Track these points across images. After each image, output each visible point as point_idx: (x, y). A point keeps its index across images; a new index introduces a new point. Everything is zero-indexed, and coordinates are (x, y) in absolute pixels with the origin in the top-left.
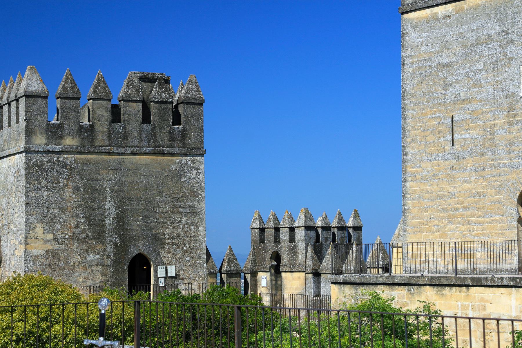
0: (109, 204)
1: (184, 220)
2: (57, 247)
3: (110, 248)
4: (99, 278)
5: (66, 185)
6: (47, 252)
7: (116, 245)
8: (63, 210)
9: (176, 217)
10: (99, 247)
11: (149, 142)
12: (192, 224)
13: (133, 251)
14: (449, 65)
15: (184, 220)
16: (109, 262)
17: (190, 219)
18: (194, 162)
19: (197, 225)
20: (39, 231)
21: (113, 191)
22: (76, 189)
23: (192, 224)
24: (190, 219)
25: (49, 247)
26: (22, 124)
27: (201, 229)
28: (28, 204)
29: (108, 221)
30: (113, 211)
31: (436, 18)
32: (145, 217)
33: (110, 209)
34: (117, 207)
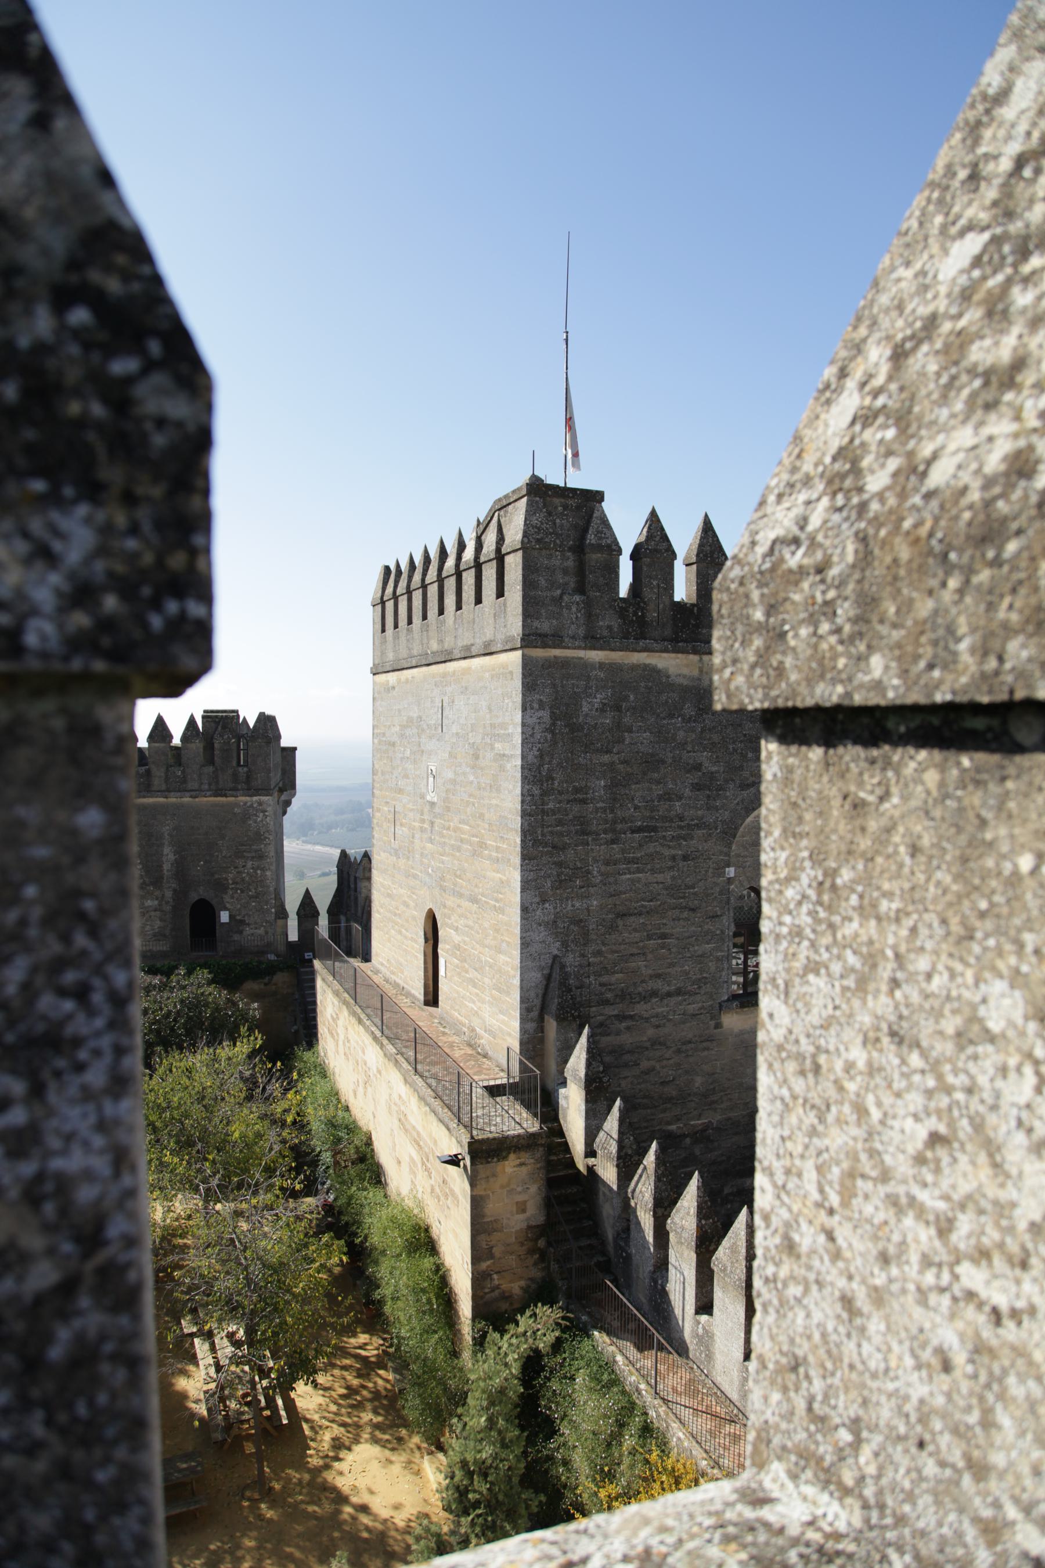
0: (167, 850)
1: (250, 864)
3: (169, 894)
4: (158, 923)
7: (175, 891)
9: (240, 862)
10: (157, 893)
11: (210, 784)
12: (258, 868)
13: (194, 897)
15: (250, 864)
16: (168, 908)
17: (256, 864)
19: (263, 870)
21: (171, 835)
23: (258, 868)
24: (256, 864)
27: (268, 873)
29: (166, 867)
32: (206, 862)
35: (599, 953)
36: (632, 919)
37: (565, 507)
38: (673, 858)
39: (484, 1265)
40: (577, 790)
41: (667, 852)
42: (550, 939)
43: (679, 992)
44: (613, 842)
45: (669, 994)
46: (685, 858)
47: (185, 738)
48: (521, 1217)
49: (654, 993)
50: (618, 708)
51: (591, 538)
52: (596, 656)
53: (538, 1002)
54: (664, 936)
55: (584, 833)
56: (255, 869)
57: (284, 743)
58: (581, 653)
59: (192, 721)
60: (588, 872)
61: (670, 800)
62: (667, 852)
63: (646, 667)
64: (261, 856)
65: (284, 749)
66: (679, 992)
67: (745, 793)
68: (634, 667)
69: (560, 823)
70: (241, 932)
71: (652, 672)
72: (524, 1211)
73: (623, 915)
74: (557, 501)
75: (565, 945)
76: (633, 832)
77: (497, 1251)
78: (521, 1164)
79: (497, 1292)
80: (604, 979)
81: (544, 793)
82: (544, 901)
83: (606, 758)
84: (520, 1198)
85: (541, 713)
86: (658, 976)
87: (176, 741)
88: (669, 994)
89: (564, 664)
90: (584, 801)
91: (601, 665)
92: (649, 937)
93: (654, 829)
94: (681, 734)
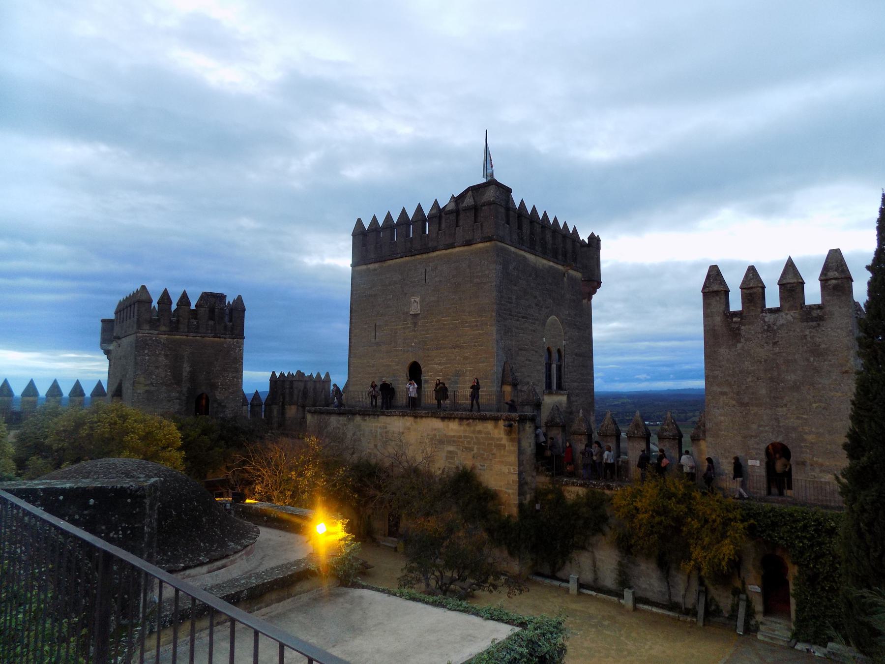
2: (153, 388)
3: (185, 390)
4: (177, 407)
6: (147, 391)
8: (157, 367)
14: (375, 295)
16: (184, 398)
18: (238, 343)
20: (142, 379)
22: (166, 356)
25: (147, 388)
26: (135, 319)
28: (136, 363)
29: (185, 374)
30: (188, 369)
31: (368, 269)
33: (186, 368)
34: (190, 367)
47: (196, 306)
52: (513, 249)
68: (521, 256)
73: (521, 350)
81: (502, 297)
83: (515, 288)
87: (193, 307)
90: (510, 303)
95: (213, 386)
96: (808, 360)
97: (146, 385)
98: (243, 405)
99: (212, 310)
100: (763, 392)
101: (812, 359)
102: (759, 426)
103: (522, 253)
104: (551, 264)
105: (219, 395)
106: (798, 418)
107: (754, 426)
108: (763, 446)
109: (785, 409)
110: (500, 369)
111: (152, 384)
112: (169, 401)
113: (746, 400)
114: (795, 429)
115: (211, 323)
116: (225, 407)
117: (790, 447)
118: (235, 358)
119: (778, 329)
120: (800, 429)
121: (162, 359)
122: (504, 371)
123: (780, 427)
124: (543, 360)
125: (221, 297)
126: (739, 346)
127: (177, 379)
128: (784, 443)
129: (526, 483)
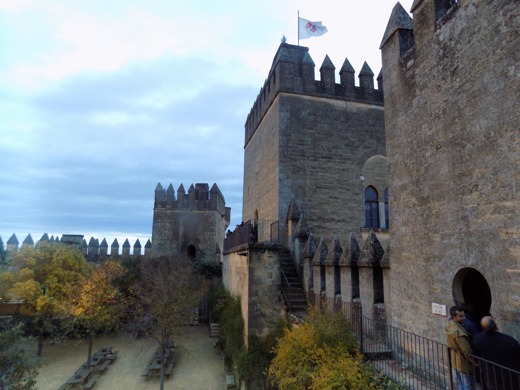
2: (162, 242)
3: (180, 243)
5: (167, 221)
6: (159, 244)
8: (165, 230)
10: (177, 242)
13: (189, 245)
15: (208, 233)
16: (180, 248)
17: (210, 233)
18: (213, 213)
19: (213, 235)
22: (170, 223)
24: (210, 233)
25: (159, 242)
29: (180, 233)
35: (310, 200)
36: (323, 190)
37: (295, 52)
38: (339, 170)
39: (254, 299)
40: (300, 141)
41: (336, 167)
42: (290, 192)
43: (343, 221)
44: (315, 160)
45: (339, 221)
46: (344, 170)
47: (189, 191)
48: (270, 279)
49: (333, 220)
50: (315, 115)
51: (304, 60)
53: (286, 216)
54: (336, 198)
55: (303, 156)
56: (210, 235)
57: (226, 206)
58: (301, 96)
59: (192, 186)
60: (305, 170)
61: (337, 148)
62: (336, 167)
63: (325, 102)
64: (212, 231)
65: (226, 208)
66: (343, 221)
67: (366, 150)
68: (321, 102)
69: (294, 151)
70: (204, 257)
71: (329, 104)
72: (271, 277)
74: (292, 50)
75: (296, 195)
76: (322, 158)
77: (260, 293)
78: (270, 257)
79: (259, 312)
80: (313, 211)
81: (288, 140)
82: (288, 178)
83: (311, 131)
84: (270, 271)
85: (286, 113)
86: (335, 213)
87: (187, 193)
88: (339, 221)
89: (295, 99)
90: (303, 145)
91: (309, 100)
92: (330, 197)
93: (331, 158)
94: (340, 127)
95: (198, 241)
96: (505, 75)
97: (158, 240)
98: (217, 253)
99: (197, 194)
100: (445, 170)
101: (512, 70)
102: (443, 237)
103: (324, 100)
104: (373, 107)
105: (201, 246)
106: (497, 210)
107: (437, 238)
108: (450, 276)
109: (475, 195)
110: (285, 206)
111: (162, 239)
112: (171, 250)
113: (426, 192)
114: (494, 236)
115: (196, 201)
116: (205, 254)
117: (488, 276)
118: (212, 223)
119: (456, 44)
120: (503, 236)
121: (168, 224)
122: (290, 207)
123: (469, 234)
124: (362, 198)
125: (205, 186)
126: (415, 101)
127: (176, 235)
128: (479, 268)
129: (263, 315)
